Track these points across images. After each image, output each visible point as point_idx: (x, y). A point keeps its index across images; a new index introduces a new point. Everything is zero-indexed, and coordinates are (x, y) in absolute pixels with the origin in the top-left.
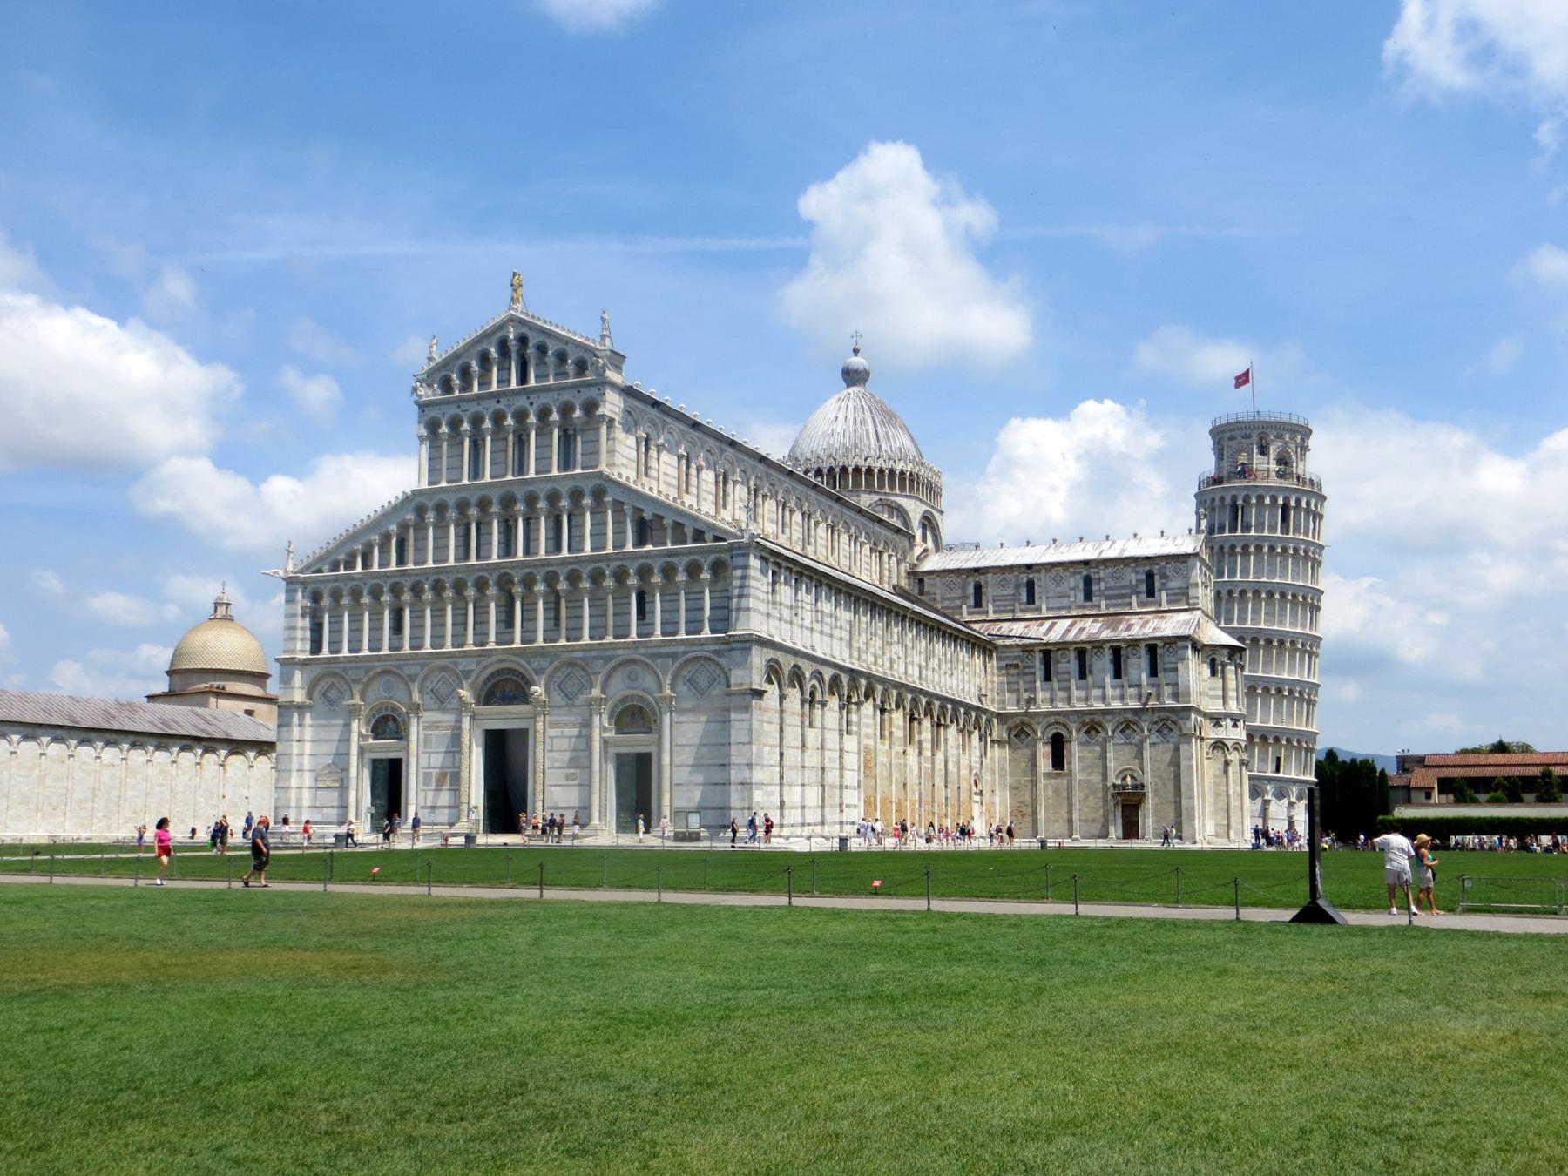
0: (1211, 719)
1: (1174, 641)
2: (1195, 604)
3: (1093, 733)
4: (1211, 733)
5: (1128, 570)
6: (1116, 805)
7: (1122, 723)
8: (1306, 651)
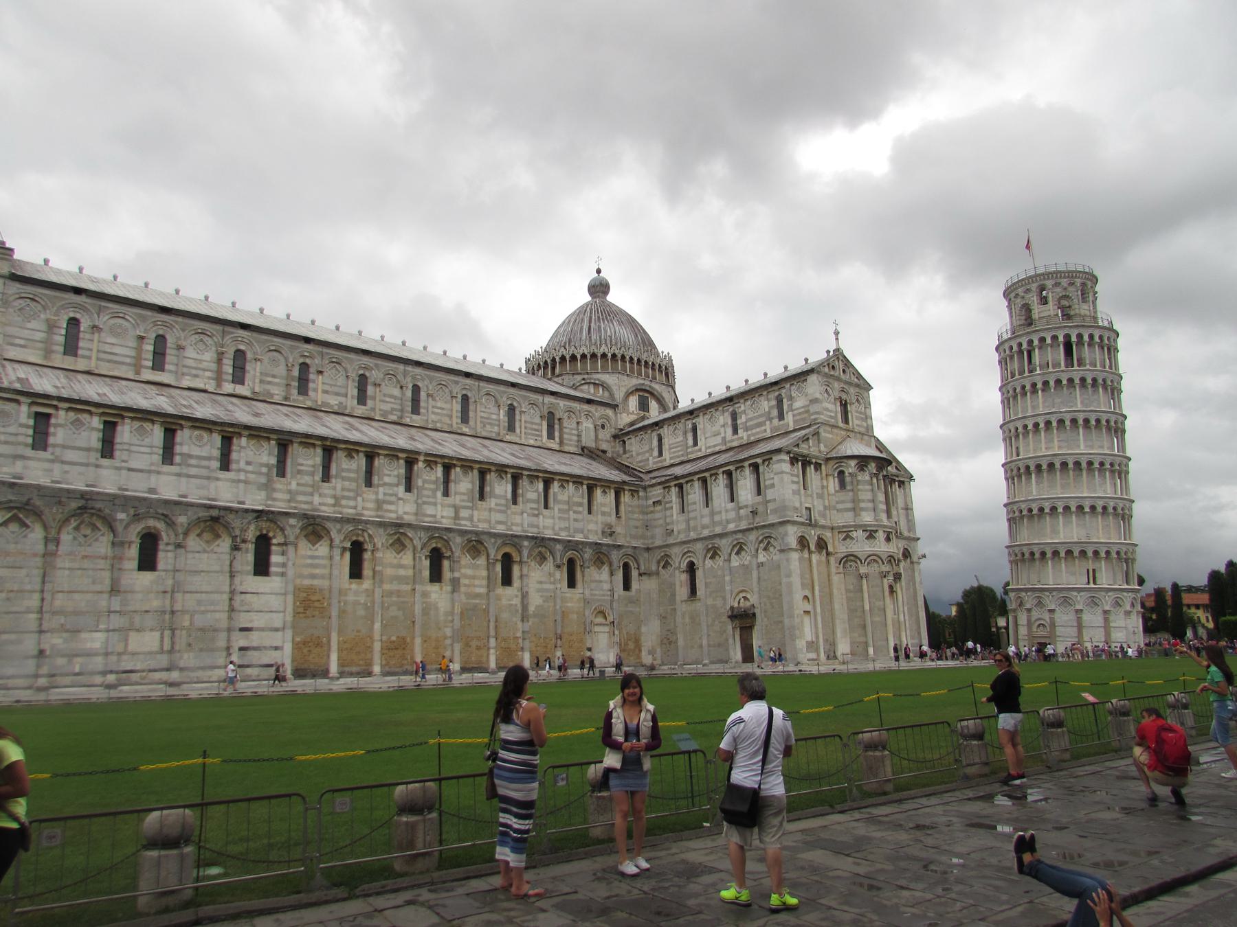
0: (839, 532)
1: (768, 456)
2: (815, 419)
3: (717, 557)
4: (840, 548)
5: (762, 398)
6: (733, 628)
7: (734, 546)
8: (1105, 469)
